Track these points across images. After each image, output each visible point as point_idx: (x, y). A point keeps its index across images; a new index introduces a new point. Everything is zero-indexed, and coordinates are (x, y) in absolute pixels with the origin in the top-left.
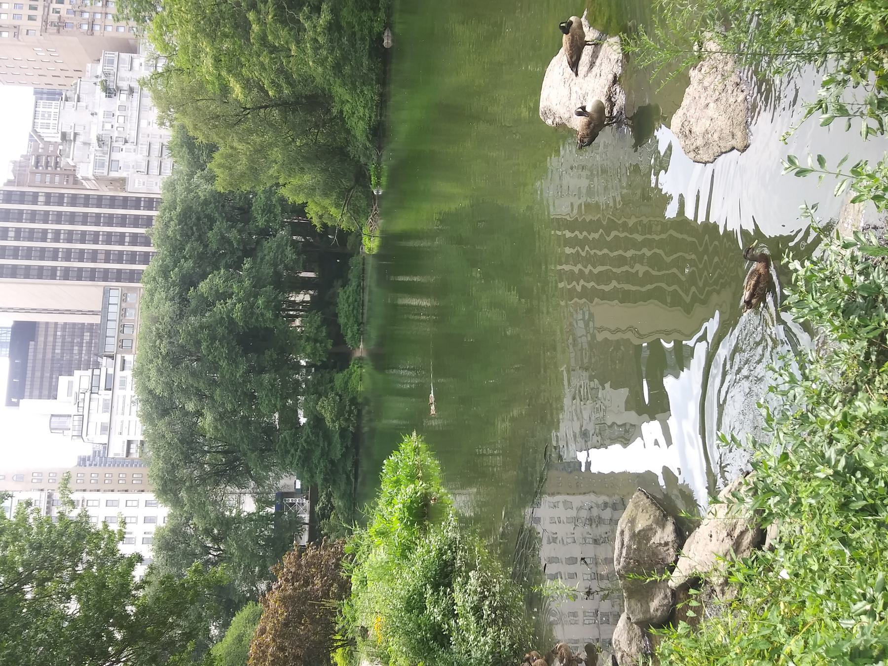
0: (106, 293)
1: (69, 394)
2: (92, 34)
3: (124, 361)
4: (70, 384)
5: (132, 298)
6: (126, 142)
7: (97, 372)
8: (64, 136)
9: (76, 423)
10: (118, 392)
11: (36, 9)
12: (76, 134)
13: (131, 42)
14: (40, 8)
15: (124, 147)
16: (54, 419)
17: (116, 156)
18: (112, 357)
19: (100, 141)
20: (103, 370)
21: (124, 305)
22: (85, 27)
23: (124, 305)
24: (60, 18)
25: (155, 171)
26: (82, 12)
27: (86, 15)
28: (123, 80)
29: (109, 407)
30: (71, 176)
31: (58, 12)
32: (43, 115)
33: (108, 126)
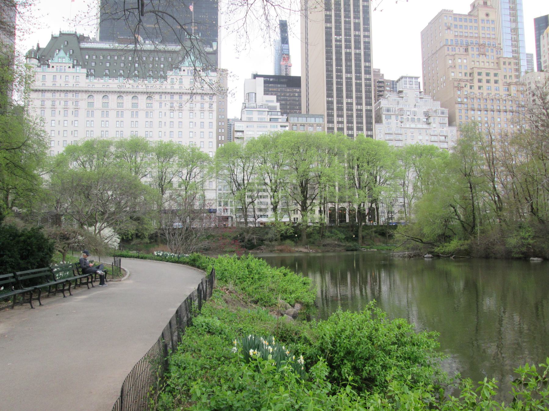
0: (321, 116)
1: (267, 101)
2: (456, 103)
3: (285, 127)
4: (272, 101)
5: (319, 129)
6: (401, 122)
7: (279, 114)
8: (401, 92)
9: (252, 105)
10: (269, 125)
11: (465, 76)
12: (403, 97)
13: (454, 123)
14: (466, 78)
15: (398, 121)
16: (254, 94)
17: (393, 117)
18: (287, 120)
19: (401, 110)
20: (281, 117)
21: (315, 125)
22: (459, 100)
23: (315, 125)
24: (463, 87)
25: (388, 137)
26: (467, 98)
27: (465, 100)
28: (434, 119)
29: (261, 121)
30: (380, 95)
31: (465, 86)
32: (411, 81)
33: (408, 113)
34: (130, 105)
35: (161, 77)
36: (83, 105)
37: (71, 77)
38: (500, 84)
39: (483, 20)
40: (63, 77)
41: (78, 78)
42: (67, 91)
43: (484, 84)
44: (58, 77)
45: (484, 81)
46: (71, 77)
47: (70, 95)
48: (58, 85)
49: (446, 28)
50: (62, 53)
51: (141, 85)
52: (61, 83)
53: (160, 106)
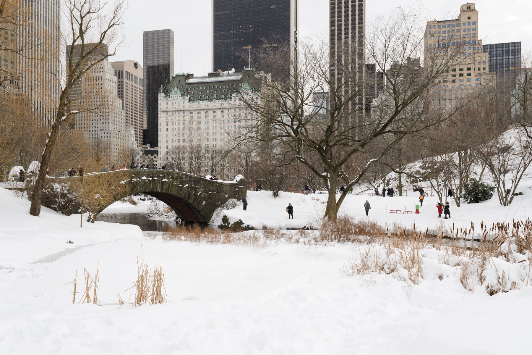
34: (212, 117)
35: (229, 98)
36: (187, 118)
37: (181, 102)
38: (473, 77)
39: (464, 24)
40: (177, 103)
41: (184, 103)
42: (179, 111)
43: (457, 78)
44: (174, 103)
45: (458, 76)
46: (181, 102)
47: (181, 113)
48: (174, 107)
49: (430, 36)
50: (176, 89)
51: (218, 104)
52: (175, 105)
53: (229, 116)
